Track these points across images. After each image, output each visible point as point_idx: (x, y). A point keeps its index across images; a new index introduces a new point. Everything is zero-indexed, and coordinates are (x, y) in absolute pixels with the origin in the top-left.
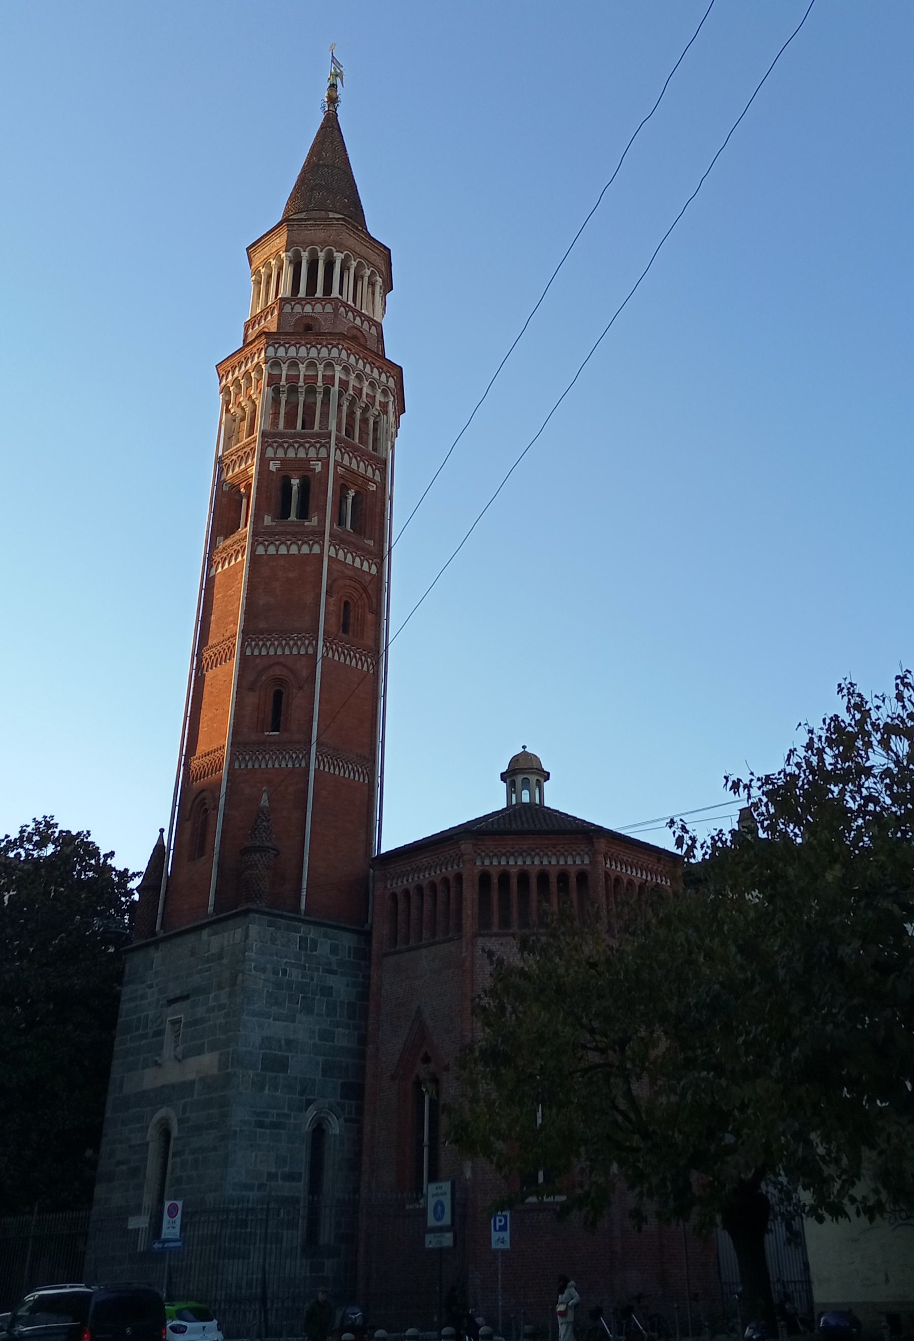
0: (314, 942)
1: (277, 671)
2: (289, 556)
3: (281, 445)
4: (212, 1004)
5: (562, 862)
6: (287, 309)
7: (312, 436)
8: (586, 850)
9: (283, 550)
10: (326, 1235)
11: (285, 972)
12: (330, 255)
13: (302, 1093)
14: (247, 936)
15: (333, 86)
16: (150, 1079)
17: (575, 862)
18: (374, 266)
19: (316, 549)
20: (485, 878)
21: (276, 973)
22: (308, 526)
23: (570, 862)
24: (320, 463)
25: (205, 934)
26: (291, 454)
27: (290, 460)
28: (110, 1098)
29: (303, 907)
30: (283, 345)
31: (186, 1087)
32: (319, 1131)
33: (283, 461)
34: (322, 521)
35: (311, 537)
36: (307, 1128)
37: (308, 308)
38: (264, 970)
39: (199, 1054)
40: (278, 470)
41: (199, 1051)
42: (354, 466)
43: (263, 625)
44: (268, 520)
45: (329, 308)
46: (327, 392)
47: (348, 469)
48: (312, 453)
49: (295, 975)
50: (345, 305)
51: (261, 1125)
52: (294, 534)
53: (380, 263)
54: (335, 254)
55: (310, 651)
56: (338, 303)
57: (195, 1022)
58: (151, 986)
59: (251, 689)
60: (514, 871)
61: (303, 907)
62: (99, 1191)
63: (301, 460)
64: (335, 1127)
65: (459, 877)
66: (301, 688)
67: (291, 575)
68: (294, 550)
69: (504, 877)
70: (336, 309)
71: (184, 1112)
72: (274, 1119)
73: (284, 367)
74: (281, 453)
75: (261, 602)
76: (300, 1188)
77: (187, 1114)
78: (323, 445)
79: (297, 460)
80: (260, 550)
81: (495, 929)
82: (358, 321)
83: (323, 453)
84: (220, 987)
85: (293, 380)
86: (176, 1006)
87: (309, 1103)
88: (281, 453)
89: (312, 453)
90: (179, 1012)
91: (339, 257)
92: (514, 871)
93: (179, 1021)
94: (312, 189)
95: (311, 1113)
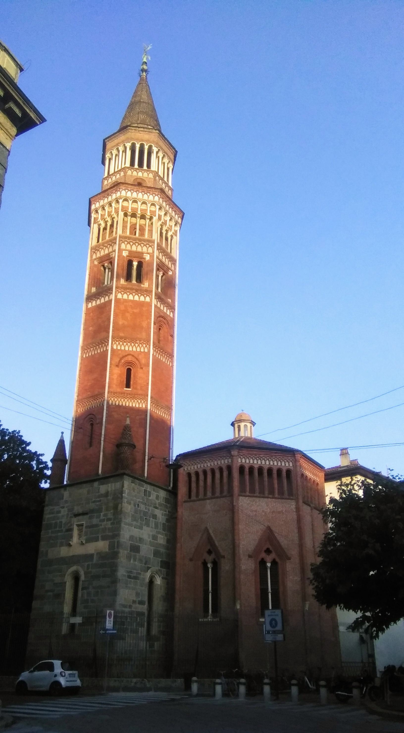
0: (150, 492)
1: (130, 358)
2: (133, 301)
3: (129, 243)
4: (102, 517)
5: (279, 464)
6: (129, 172)
7: (145, 240)
8: (291, 460)
9: (131, 297)
10: (155, 631)
11: (138, 505)
13: (145, 564)
14: (123, 486)
16: (64, 552)
17: (285, 464)
18: (170, 158)
19: (148, 299)
20: (242, 469)
21: (135, 506)
22: (143, 287)
23: (283, 464)
24: (149, 255)
25: (96, 484)
26: (134, 248)
28: (40, 561)
29: (146, 475)
30: (130, 191)
31: (89, 557)
32: (151, 582)
33: (130, 252)
34: (150, 285)
35: (145, 293)
36: (147, 580)
37: (140, 174)
38: (130, 504)
39: (96, 541)
40: (127, 256)
41: (96, 540)
42: (164, 260)
43: (122, 334)
44: (122, 281)
45: (151, 176)
46: (151, 218)
47: (161, 261)
48: (145, 249)
49: (142, 507)
50: (159, 176)
51: (129, 577)
52: (137, 290)
53: (172, 157)
55: (146, 350)
56: (156, 174)
57: (92, 526)
58: (63, 507)
59: (117, 366)
60: (256, 466)
61: (146, 475)
62: (35, 604)
63: (139, 252)
64: (158, 581)
65: (229, 468)
66: (142, 368)
67: (135, 311)
68: (136, 298)
69: (251, 469)
70: (155, 177)
71: (88, 568)
72: (135, 575)
74: (129, 247)
75: (121, 323)
76: (144, 608)
77: (90, 570)
78: (150, 246)
79: (136, 252)
80: (119, 296)
81: (248, 493)
82: (164, 186)
83: (150, 250)
84: (107, 510)
86: (81, 517)
87: (148, 568)
88: (129, 247)
89: (145, 249)
90: (84, 521)
91: (155, 149)
92: (256, 466)
93: (82, 525)
94: (139, 113)
95: (148, 574)
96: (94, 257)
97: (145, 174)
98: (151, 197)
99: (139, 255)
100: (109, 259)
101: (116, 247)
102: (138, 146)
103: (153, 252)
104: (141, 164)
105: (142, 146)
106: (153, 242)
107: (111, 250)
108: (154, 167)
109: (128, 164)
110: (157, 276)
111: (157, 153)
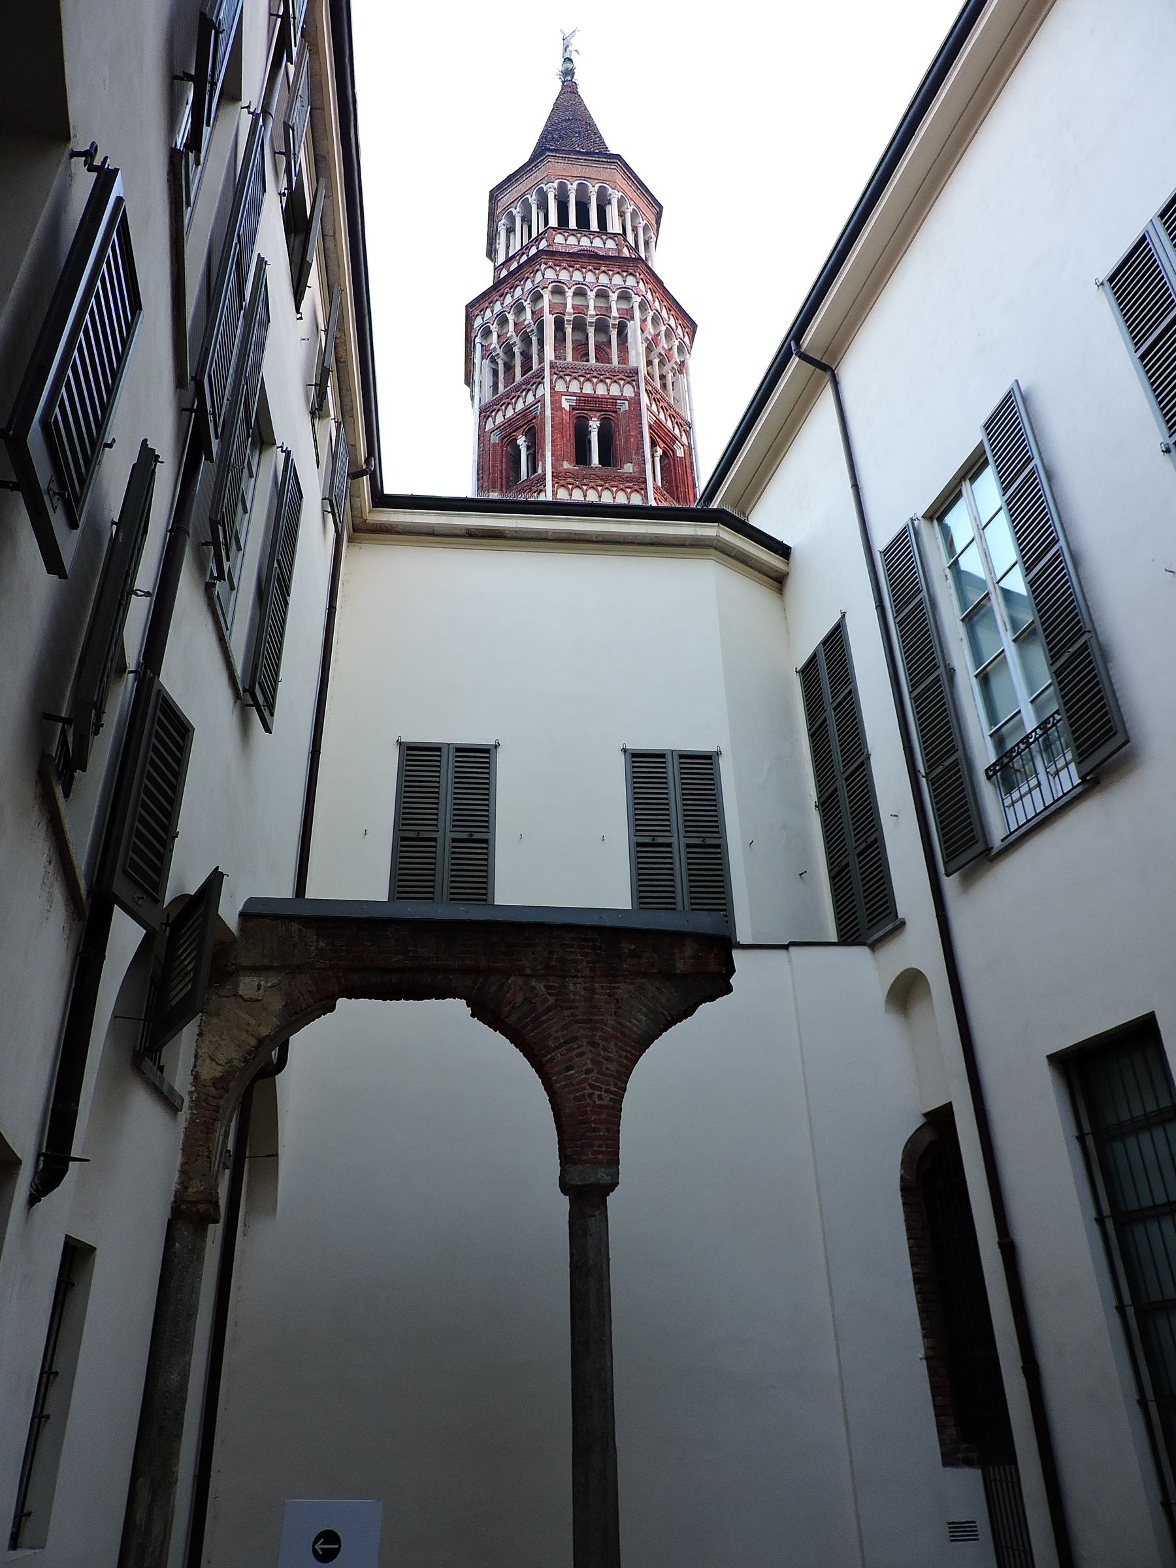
12: (602, 194)
26: (588, 389)
27: (588, 396)
54: (611, 191)
74: (575, 387)
85: (580, 310)
88: (575, 387)
91: (615, 196)
96: (490, 425)
97: (598, 242)
98: (617, 280)
99: (605, 407)
101: (545, 390)
102: (572, 188)
103: (638, 394)
104: (583, 221)
105: (582, 191)
106: (636, 372)
107: (530, 398)
108: (614, 226)
109: (553, 221)
110: (653, 456)
111: (621, 202)
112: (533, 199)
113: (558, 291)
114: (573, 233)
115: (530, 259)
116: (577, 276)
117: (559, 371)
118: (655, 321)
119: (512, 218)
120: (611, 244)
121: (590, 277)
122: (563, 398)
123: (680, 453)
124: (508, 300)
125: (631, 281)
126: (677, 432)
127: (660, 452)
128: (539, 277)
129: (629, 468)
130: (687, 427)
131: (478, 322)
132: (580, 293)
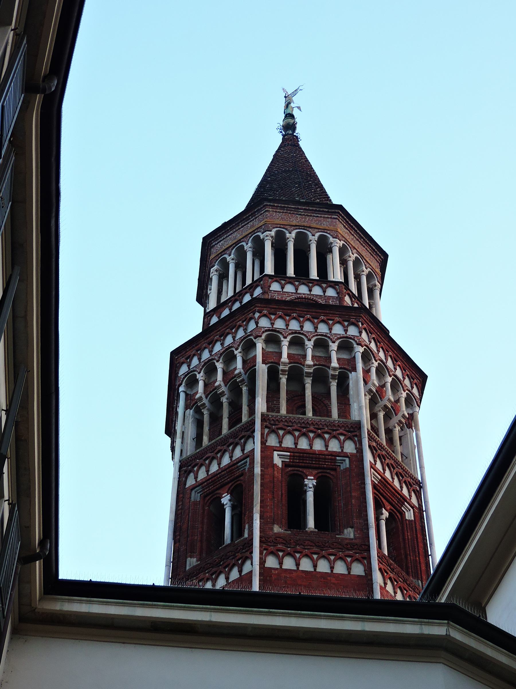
15: (289, 116)
19: (358, 569)
24: (347, 460)
26: (303, 444)
27: (303, 451)
47: (384, 478)
54: (331, 239)
73: (285, 343)
74: (288, 442)
80: (271, 562)
85: (297, 361)
88: (288, 442)
91: (337, 244)
96: (191, 481)
97: (317, 291)
98: (338, 329)
99: (322, 464)
100: (236, 478)
102: (291, 236)
103: (360, 450)
107: (238, 453)
108: (336, 274)
109: (269, 269)
110: (378, 520)
111: (343, 251)
112: (248, 247)
113: (273, 339)
114: (290, 281)
115: (244, 308)
116: (294, 325)
117: (271, 424)
118: (381, 371)
119: (225, 265)
120: (331, 292)
121: (308, 327)
122: (276, 453)
123: (409, 515)
124: (218, 348)
125: (352, 331)
126: (405, 492)
127: (385, 514)
128: (252, 326)
129: (349, 533)
130: (418, 487)
131: (184, 369)
132: (297, 342)
